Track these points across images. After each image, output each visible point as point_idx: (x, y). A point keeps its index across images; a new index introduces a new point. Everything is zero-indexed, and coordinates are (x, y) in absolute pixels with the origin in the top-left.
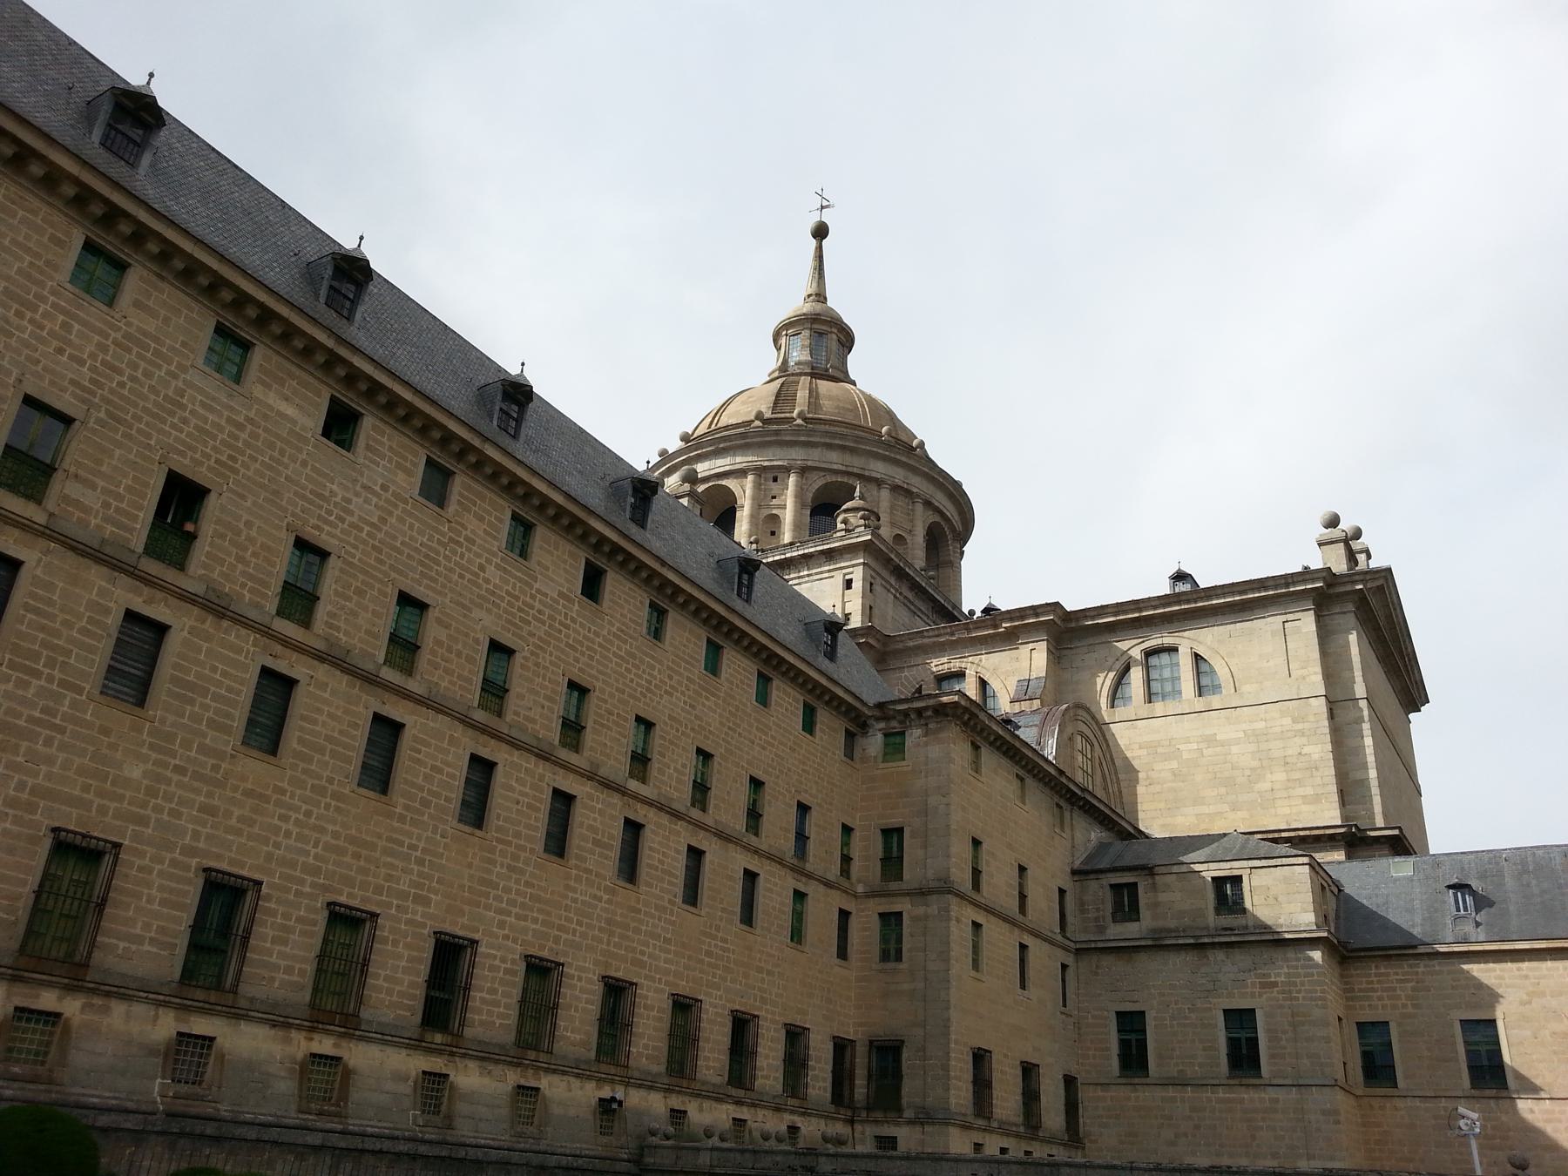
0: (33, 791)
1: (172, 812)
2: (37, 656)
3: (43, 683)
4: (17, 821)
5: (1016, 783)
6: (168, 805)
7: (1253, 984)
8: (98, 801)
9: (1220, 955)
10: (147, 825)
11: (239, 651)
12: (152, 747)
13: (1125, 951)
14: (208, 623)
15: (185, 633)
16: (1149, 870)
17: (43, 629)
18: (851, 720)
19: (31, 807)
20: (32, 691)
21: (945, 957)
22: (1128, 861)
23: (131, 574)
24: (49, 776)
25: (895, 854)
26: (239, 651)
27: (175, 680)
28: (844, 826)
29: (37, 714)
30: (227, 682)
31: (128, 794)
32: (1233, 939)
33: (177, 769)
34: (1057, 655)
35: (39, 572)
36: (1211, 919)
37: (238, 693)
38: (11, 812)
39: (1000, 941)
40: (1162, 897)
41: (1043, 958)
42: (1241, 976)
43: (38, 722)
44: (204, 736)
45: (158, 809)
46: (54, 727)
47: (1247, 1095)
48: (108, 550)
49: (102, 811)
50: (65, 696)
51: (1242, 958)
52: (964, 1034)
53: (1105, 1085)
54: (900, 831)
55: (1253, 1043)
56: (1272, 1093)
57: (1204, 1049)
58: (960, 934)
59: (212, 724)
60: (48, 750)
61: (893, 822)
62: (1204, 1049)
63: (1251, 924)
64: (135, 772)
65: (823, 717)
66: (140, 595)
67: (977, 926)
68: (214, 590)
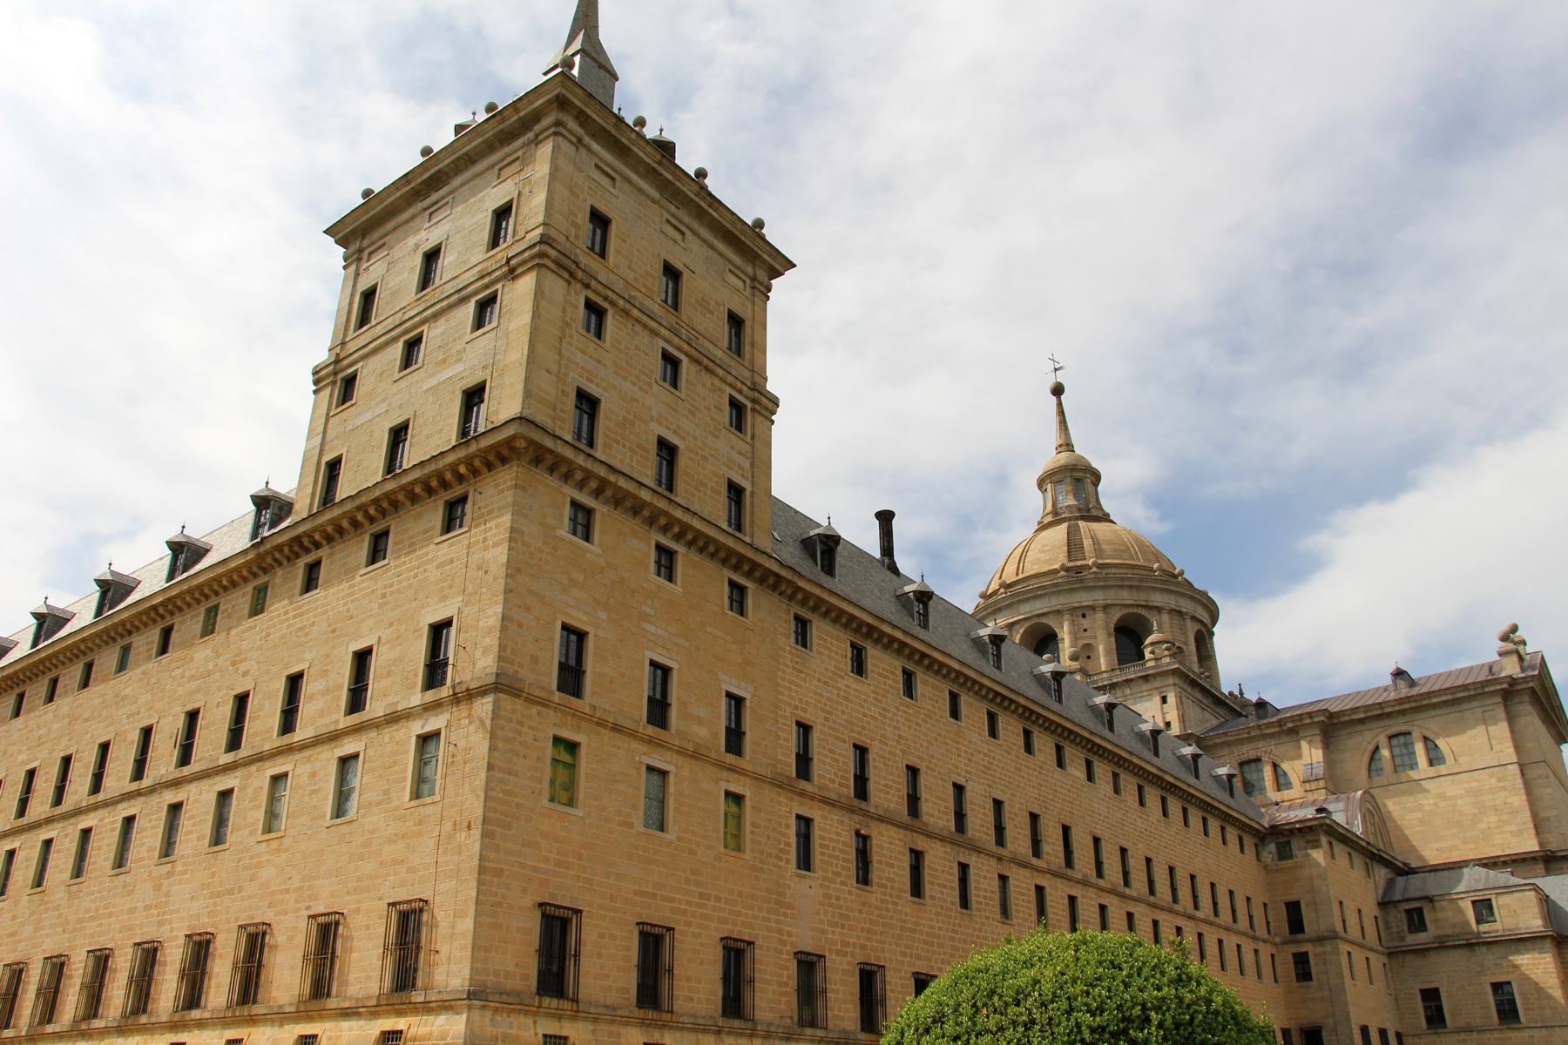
13: (1422, 951)
16: (1430, 899)
21: (1340, 976)
22: (1412, 893)
34: (1328, 744)
40: (1440, 915)
41: (1377, 961)
47: (1513, 1034)
52: (1356, 1022)
53: (1419, 1036)
55: (1512, 1002)
56: (1529, 1032)
58: (1344, 959)
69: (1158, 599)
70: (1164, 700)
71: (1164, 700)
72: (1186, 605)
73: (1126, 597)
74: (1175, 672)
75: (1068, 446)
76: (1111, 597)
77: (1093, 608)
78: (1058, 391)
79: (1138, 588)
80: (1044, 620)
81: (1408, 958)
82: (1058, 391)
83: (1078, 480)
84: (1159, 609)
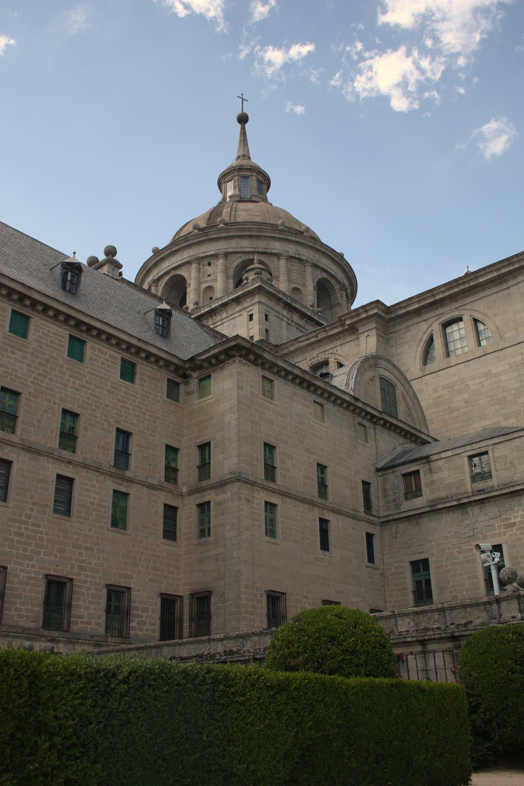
5: (318, 408)
7: (500, 527)
9: (476, 509)
18: (172, 372)
25: (207, 462)
28: (168, 447)
32: (483, 496)
36: (468, 486)
39: (298, 521)
42: (491, 522)
51: (491, 510)
54: (208, 444)
57: (469, 578)
61: (204, 440)
62: (469, 578)
63: (495, 484)
65: (143, 369)
67: (270, 507)
69: (277, 247)
70: (251, 317)
71: (251, 317)
72: (305, 253)
73: (246, 245)
74: (259, 289)
75: (246, 156)
76: (232, 245)
77: (215, 256)
78: (243, 119)
79: (257, 237)
80: (179, 272)
81: (402, 526)
82: (243, 119)
83: (246, 177)
84: (278, 256)
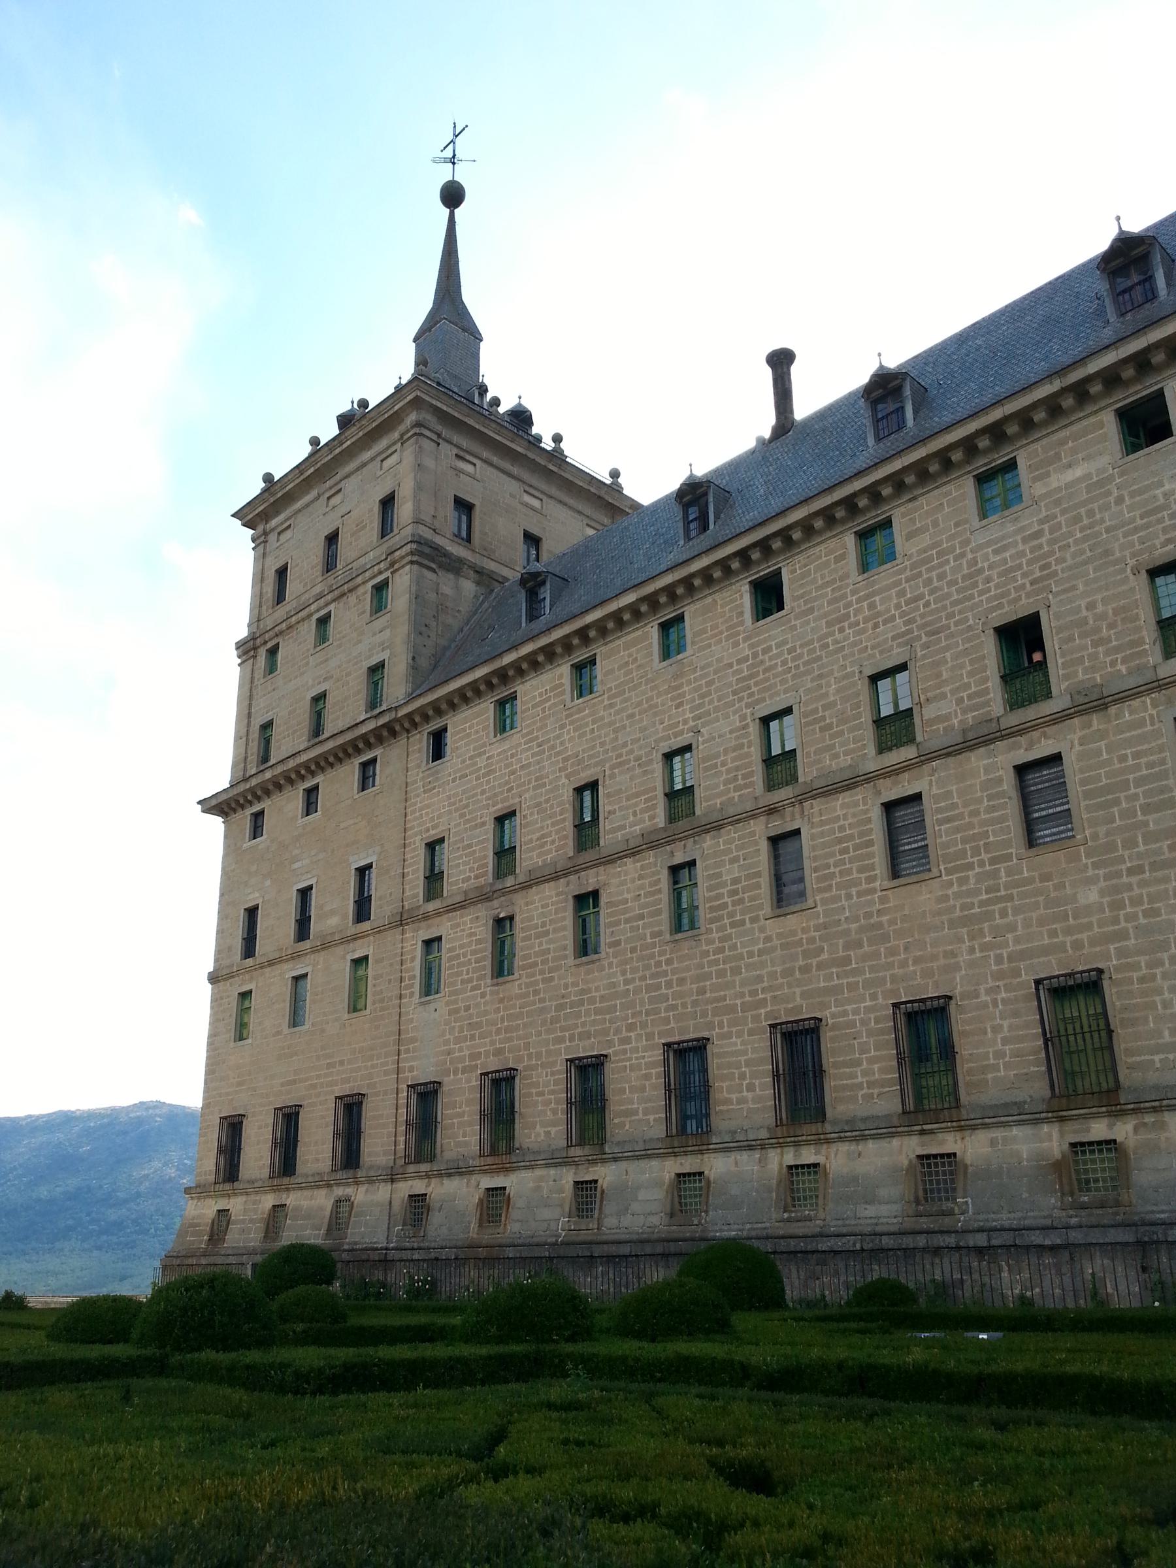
0: (1011, 959)
1: (1146, 914)
2: (964, 851)
3: (977, 870)
4: (1008, 988)
6: (1139, 909)
8: (1068, 939)
10: (1127, 938)
11: (1141, 723)
12: (1096, 866)
14: (1095, 722)
15: (1077, 748)
17: (958, 830)
19: (1016, 973)
20: (972, 881)
23: (1003, 738)
24: (1017, 941)
26: (1141, 723)
27: (1088, 795)
29: (985, 897)
30: (1143, 760)
31: (1094, 919)
33: (1131, 872)
35: (935, 791)
37: (1163, 762)
38: (1001, 983)
43: (988, 902)
44: (1146, 824)
45: (1130, 918)
46: (1000, 899)
48: (971, 735)
49: (1078, 945)
50: (999, 870)
59: (1147, 809)
60: (1005, 920)
64: (1091, 896)
66: (1020, 747)
68: (1079, 693)
